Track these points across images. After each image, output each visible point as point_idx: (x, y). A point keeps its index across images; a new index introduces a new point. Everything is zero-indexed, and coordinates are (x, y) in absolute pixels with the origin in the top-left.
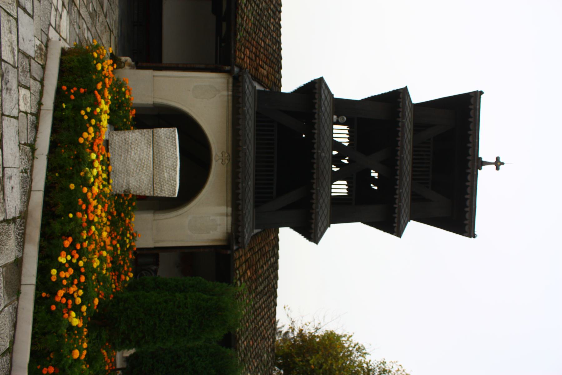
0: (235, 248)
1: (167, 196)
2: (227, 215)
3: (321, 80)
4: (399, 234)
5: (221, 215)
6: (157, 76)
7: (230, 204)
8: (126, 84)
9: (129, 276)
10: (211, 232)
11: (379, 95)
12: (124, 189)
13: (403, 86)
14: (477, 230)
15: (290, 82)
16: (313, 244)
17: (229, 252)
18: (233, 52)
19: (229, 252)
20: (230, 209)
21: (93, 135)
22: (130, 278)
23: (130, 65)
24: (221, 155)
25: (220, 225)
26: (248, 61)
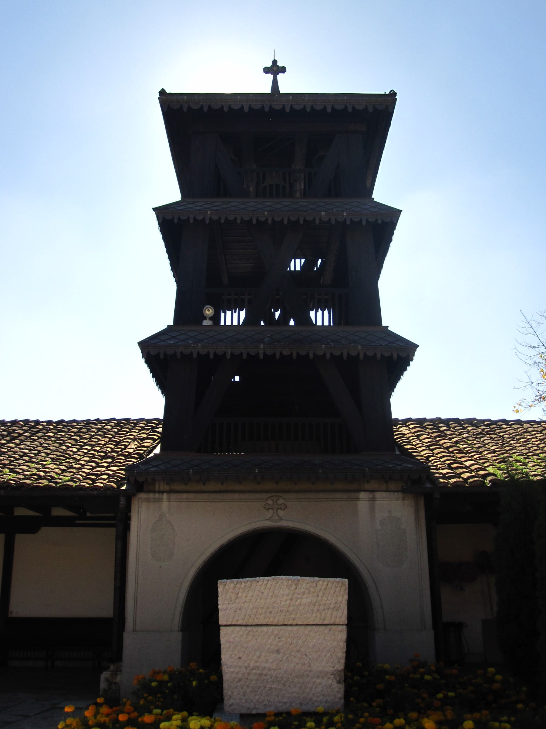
0: (428, 485)
1: (346, 597)
2: (373, 499)
3: (143, 344)
5: (372, 509)
6: (135, 624)
8: (144, 679)
9: (494, 674)
11: (170, 258)
12: (335, 684)
13: (153, 216)
14: (384, 90)
17: (437, 495)
18: (95, 492)
19: (437, 495)
20: (362, 495)
23: (115, 673)
24: (271, 511)
25: (390, 512)
26: (115, 468)
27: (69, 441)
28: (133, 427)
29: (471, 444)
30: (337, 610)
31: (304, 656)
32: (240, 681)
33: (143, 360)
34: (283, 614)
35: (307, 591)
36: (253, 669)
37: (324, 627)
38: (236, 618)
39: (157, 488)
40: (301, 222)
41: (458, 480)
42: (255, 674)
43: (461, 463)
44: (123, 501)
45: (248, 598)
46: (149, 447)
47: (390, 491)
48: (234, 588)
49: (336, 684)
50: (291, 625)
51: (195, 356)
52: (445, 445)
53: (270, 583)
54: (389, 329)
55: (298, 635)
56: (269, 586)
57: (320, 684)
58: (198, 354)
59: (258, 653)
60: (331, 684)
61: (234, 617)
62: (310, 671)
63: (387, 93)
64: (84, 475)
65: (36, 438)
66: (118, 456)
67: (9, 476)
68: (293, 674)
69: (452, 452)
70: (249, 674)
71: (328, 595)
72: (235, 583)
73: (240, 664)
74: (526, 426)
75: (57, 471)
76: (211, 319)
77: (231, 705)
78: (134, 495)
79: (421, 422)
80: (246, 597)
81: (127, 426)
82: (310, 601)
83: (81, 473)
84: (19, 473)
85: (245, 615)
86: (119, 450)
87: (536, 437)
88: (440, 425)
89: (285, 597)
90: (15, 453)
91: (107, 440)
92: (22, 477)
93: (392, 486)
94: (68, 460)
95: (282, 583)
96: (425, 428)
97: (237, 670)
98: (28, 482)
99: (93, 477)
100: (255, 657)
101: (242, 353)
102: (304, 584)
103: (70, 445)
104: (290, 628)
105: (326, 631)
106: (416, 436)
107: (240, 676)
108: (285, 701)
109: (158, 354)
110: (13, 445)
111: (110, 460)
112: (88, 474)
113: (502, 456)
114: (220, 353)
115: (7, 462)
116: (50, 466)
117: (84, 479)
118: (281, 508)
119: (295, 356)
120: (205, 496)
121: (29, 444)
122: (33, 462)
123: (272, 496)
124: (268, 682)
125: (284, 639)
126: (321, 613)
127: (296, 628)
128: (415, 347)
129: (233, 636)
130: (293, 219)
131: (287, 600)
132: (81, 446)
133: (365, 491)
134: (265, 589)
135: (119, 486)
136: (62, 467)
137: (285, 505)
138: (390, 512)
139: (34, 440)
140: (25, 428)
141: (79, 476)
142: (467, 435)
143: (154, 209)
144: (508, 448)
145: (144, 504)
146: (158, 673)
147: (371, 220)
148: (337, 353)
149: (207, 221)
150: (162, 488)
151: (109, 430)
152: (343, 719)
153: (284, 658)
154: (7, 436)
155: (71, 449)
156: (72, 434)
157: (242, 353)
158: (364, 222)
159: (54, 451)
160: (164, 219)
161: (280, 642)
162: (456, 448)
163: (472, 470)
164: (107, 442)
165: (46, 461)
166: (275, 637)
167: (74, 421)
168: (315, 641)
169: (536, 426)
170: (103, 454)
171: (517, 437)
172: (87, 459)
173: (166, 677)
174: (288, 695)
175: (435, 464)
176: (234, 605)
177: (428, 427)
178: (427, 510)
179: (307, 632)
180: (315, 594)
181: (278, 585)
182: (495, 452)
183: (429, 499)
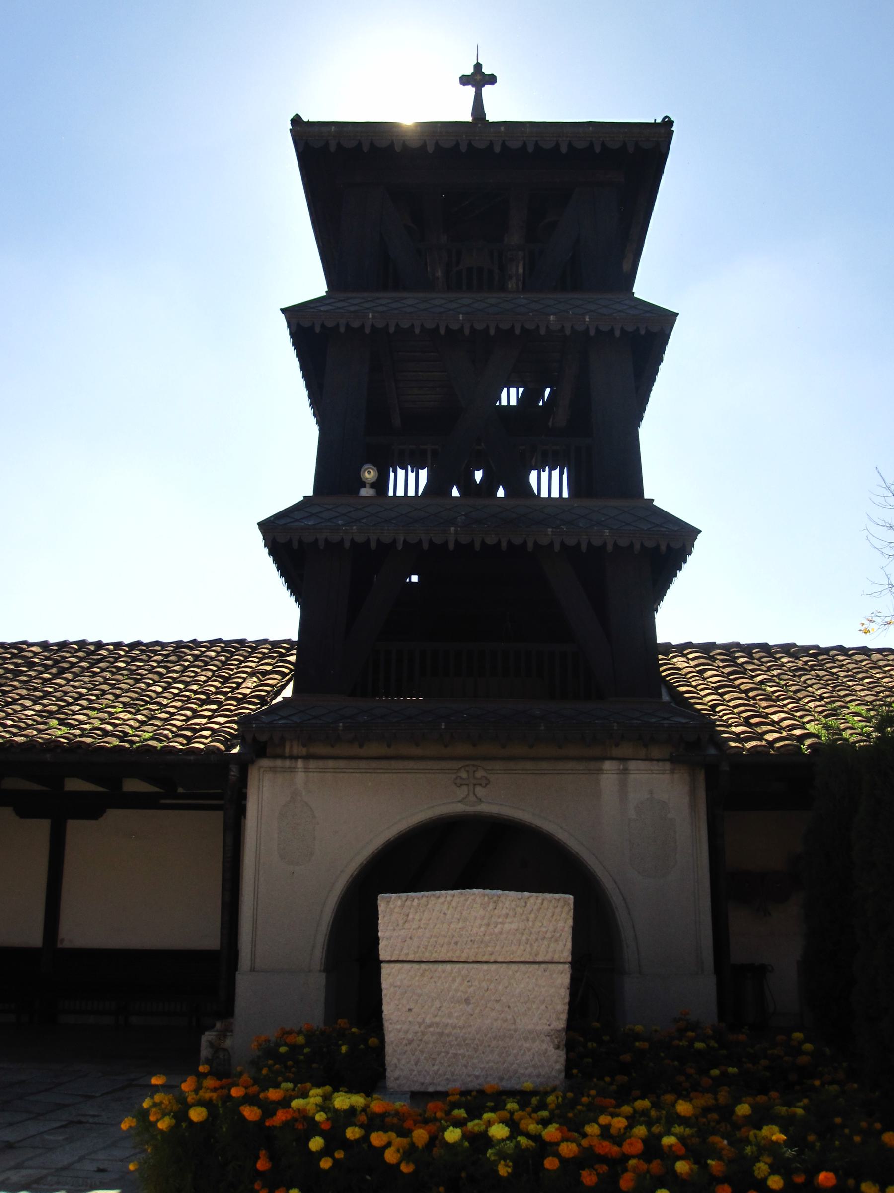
0: (712, 751)
1: (570, 922)
2: (625, 772)
4: (666, 319)
5: (623, 786)
6: (253, 960)
8: (268, 1041)
9: (801, 1043)
11: (308, 386)
12: (551, 1050)
15: (271, 612)
16: (699, 543)
17: (725, 767)
18: (192, 758)
19: (725, 767)
20: (608, 765)
21: (393, 1135)
22: (807, 1040)
23: (223, 1034)
24: (465, 788)
26: (222, 720)
27: (150, 675)
28: (251, 654)
29: (785, 685)
30: (556, 941)
31: (507, 1009)
32: (410, 1044)
33: (266, 551)
35: (511, 913)
36: (430, 1027)
37: (536, 966)
38: (405, 951)
39: (287, 750)
40: (517, 331)
41: (759, 743)
42: (433, 1034)
43: (766, 716)
44: (234, 772)
45: (423, 921)
46: (275, 686)
47: (651, 760)
48: (403, 906)
50: (487, 962)
51: (347, 545)
52: (742, 687)
53: (456, 899)
54: (654, 503)
56: (454, 904)
57: (529, 1050)
58: (352, 541)
59: (437, 1004)
60: (546, 1050)
61: (402, 950)
62: (515, 1031)
63: (659, 121)
64: (174, 729)
65: (99, 670)
68: (489, 1035)
69: (754, 698)
70: (423, 1034)
71: (544, 918)
72: (404, 899)
73: (410, 1019)
74: (875, 656)
75: (131, 723)
76: (373, 485)
77: (397, 1079)
78: (253, 762)
79: (707, 649)
81: (241, 652)
82: (516, 927)
83: (169, 727)
85: (419, 947)
86: (228, 690)
88: (737, 654)
89: (478, 921)
90: (65, 693)
91: (209, 674)
92: (78, 732)
93: (655, 752)
94: (148, 706)
95: (474, 900)
96: (713, 659)
97: (405, 1027)
98: (89, 740)
99: (189, 733)
100: (433, 1008)
101: (420, 541)
102: (507, 903)
103: (151, 682)
104: (485, 967)
105: (540, 973)
106: (697, 672)
107: (410, 1036)
108: (477, 1073)
109: (290, 541)
110: (63, 682)
111: (214, 707)
112: (180, 728)
113: (834, 705)
115: (54, 708)
116: (122, 715)
117: (174, 737)
118: (480, 785)
119: (504, 545)
120: (363, 764)
121: (87, 679)
122: (94, 709)
123: (467, 765)
124: (452, 1046)
125: (476, 983)
126: (531, 945)
129: (399, 977)
130: (505, 326)
132: (169, 683)
133: (612, 758)
134: (448, 908)
135: (229, 748)
136: (139, 717)
137: (486, 778)
139: (95, 674)
140: (80, 654)
141: (166, 732)
143: (283, 311)
144: (842, 693)
146: (290, 1033)
147: (630, 328)
148: (571, 542)
149: (367, 330)
150: (295, 751)
151: (212, 658)
152: (560, 1099)
153: (477, 1011)
154: (52, 666)
155: (153, 688)
157: (420, 541)
158: (617, 333)
159: (127, 691)
160: (298, 324)
161: (470, 987)
162: (759, 692)
164: (209, 678)
165: (114, 707)
167: (157, 643)
168: (522, 986)
170: (203, 697)
171: (860, 676)
172: (179, 704)
173: (301, 1040)
174: (482, 1066)
175: (725, 718)
176: (402, 932)
177: (719, 657)
178: (709, 789)
179: (510, 973)
180: (524, 917)
181: (468, 902)
182: (821, 698)
183: (712, 772)
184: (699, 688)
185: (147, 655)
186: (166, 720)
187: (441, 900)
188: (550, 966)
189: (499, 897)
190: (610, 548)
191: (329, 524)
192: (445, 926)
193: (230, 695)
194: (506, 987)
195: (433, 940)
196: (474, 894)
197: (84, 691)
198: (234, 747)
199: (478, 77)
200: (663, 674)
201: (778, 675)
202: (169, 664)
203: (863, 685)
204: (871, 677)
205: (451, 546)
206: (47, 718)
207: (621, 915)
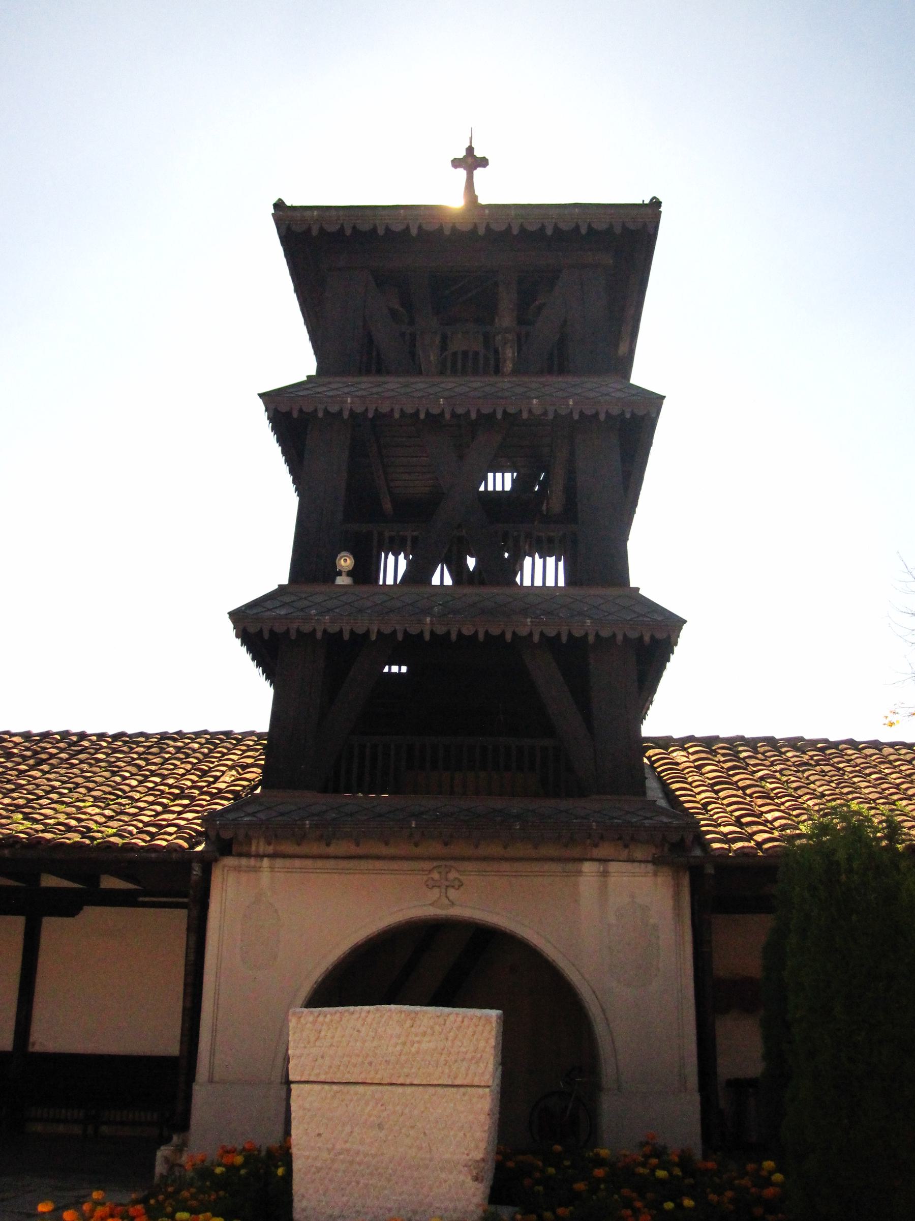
0: (698, 852)
2: (605, 874)
3: (235, 615)
5: (603, 889)
7: (570, 866)
9: (771, 1173)
10: (652, 921)
12: (469, 1180)
14: (640, 197)
16: (685, 635)
17: (710, 870)
19: (710, 870)
20: (587, 867)
22: (779, 1169)
23: (180, 1149)
24: (436, 890)
25: (633, 896)
27: (128, 768)
28: (235, 745)
29: (786, 781)
30: (477, 1063)
31: (422, 1135)
32: (318, 1172)
33: (239, 641)
34: (391, 1066)
36: (340, 1153)
37: (454, 1090)
38: (316, 1071)
39: (254, 848)
40: (499, 416)
41: (746, 844)
42: (343, 1162)
44: (197, 870)
45: (336, 1039)
46: (253, 780)
47: (633, 861)
48: (314, 1022)
49: (471, 1182)
50: (402, 1085)
51: (319, 635)
52: (740, 784)
53: (371, 1016)
54: (640, 592)
55: (413, 1101)
56: (369, 1020)
57: (445, 1181)
58: (325, 631)
59: (348, 1129)
60: (463, 1181)
62: (431, 1160)
63: (647, 202)
64: (140, 825)
65: (77, 762)
66: (199, 795)
67: (20, 826)
69: (750, 796)
70: (333, 1161)
72: (316, 1014)
74: (887, 751)
75: (97, 818)
76: (349, 574)
77: (304, 1210)
78: (216, 860)
79: (709, 743)
80: (333, 1037)
81: (225, 744)
83: (135, 823)
84: (36, 821)
86: (204, 784)
87: (900, 772)
88: (740, 749)
89: (394, 1040)
90: (38, 786)
91: (189, 767)
92: (40, 827)
93: (638, 855)
94: (119, 800)
95: (390, 1017)
96: (714, 753)
98: (48, 836)
99: (153, 830)
100: (343, 1135)
102: (425, 1021)
103: (128, 775)
104: (400, 1090)
106: (695, 767)
107: (319, 1164)
108: (389, 1206)
109: (261, 631)
111: (186, 802)
112: (147, 824)
113: (834, 803)
114: (360, 630)
115: (22, 802)
116: (89, 810)
117: (138, 833)
118: (453, 887)
119: (481, 637)
120: (331, 863)
121: (62, 771)
122: (63, 803)
126: (450, 1067)
127: (409, 1090)
128: (676, 623)
130: (486, 411)
131: (396, 1045)
132: (146, 777)
134: (363, 1025)
135: (192, 846)
136: (107, 812)
137: (460, 880)
138: (633, 896)
139: (73, 766)
140: (62, 745)
141: (131, 828)
142: (782, 766)
144: (845, 790)
145: (231, 878)
147: (615, 411)
148: (551, 632)
149: (346, 415)
150: (261, 851)
151: (194, 751)
154: (30, 757)
155: (127, 782)
156: (135, 756)
157: (394, 632)
159: (102, 784)
162: (757, 789)
163: (775, 828)
164: (188, 771)
165: (84, 801)
166: (377, 1104)
167: (142, 734)
169: (903, 751)
170: (177, 791)
171: (867, 771)
172: (151, 799)
173: (239, 1160)
175: (715, 817)
176: (314, 1050)
177: (720, 751)
179: (427, 1097)
181: (384, 1020)
182: (823, 795)
183: (696, 873)
184: (694, 784)
185: (129, 747)
186: (135, 815)
187: (356, 1016)
188: (469, 1089)
189: (416, 1013)
190: (591, 639)
191: (302, 613)
192: (359, 1044)
193: (205, 789)
194: (423, 1112)
195: (345, 1059)
196: (390, 1010)
197: (57, 784)
198: (199, 843)
199: (470, 160)
200: (659, 770)
201: (780, 771)
202: (150, 757)
203: (869, 782)
204: (880, 772)
205: (427, 637)
206: (12, 811)
207: (600, 1028)
